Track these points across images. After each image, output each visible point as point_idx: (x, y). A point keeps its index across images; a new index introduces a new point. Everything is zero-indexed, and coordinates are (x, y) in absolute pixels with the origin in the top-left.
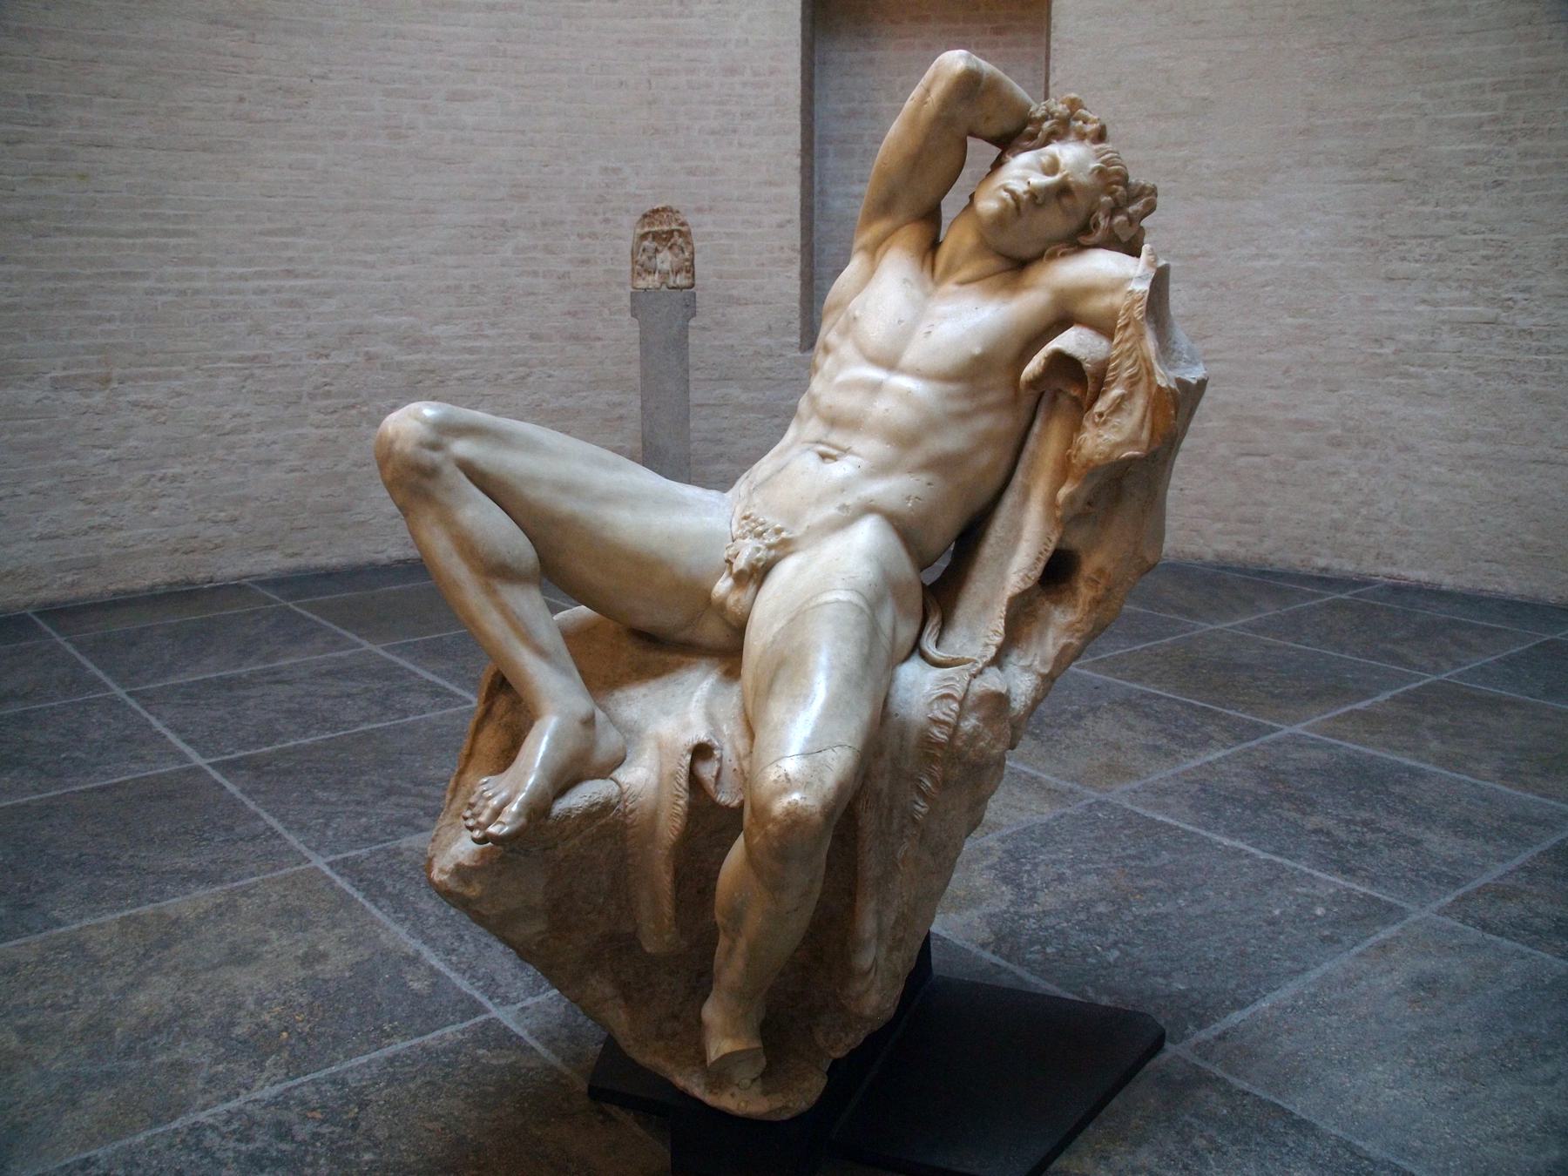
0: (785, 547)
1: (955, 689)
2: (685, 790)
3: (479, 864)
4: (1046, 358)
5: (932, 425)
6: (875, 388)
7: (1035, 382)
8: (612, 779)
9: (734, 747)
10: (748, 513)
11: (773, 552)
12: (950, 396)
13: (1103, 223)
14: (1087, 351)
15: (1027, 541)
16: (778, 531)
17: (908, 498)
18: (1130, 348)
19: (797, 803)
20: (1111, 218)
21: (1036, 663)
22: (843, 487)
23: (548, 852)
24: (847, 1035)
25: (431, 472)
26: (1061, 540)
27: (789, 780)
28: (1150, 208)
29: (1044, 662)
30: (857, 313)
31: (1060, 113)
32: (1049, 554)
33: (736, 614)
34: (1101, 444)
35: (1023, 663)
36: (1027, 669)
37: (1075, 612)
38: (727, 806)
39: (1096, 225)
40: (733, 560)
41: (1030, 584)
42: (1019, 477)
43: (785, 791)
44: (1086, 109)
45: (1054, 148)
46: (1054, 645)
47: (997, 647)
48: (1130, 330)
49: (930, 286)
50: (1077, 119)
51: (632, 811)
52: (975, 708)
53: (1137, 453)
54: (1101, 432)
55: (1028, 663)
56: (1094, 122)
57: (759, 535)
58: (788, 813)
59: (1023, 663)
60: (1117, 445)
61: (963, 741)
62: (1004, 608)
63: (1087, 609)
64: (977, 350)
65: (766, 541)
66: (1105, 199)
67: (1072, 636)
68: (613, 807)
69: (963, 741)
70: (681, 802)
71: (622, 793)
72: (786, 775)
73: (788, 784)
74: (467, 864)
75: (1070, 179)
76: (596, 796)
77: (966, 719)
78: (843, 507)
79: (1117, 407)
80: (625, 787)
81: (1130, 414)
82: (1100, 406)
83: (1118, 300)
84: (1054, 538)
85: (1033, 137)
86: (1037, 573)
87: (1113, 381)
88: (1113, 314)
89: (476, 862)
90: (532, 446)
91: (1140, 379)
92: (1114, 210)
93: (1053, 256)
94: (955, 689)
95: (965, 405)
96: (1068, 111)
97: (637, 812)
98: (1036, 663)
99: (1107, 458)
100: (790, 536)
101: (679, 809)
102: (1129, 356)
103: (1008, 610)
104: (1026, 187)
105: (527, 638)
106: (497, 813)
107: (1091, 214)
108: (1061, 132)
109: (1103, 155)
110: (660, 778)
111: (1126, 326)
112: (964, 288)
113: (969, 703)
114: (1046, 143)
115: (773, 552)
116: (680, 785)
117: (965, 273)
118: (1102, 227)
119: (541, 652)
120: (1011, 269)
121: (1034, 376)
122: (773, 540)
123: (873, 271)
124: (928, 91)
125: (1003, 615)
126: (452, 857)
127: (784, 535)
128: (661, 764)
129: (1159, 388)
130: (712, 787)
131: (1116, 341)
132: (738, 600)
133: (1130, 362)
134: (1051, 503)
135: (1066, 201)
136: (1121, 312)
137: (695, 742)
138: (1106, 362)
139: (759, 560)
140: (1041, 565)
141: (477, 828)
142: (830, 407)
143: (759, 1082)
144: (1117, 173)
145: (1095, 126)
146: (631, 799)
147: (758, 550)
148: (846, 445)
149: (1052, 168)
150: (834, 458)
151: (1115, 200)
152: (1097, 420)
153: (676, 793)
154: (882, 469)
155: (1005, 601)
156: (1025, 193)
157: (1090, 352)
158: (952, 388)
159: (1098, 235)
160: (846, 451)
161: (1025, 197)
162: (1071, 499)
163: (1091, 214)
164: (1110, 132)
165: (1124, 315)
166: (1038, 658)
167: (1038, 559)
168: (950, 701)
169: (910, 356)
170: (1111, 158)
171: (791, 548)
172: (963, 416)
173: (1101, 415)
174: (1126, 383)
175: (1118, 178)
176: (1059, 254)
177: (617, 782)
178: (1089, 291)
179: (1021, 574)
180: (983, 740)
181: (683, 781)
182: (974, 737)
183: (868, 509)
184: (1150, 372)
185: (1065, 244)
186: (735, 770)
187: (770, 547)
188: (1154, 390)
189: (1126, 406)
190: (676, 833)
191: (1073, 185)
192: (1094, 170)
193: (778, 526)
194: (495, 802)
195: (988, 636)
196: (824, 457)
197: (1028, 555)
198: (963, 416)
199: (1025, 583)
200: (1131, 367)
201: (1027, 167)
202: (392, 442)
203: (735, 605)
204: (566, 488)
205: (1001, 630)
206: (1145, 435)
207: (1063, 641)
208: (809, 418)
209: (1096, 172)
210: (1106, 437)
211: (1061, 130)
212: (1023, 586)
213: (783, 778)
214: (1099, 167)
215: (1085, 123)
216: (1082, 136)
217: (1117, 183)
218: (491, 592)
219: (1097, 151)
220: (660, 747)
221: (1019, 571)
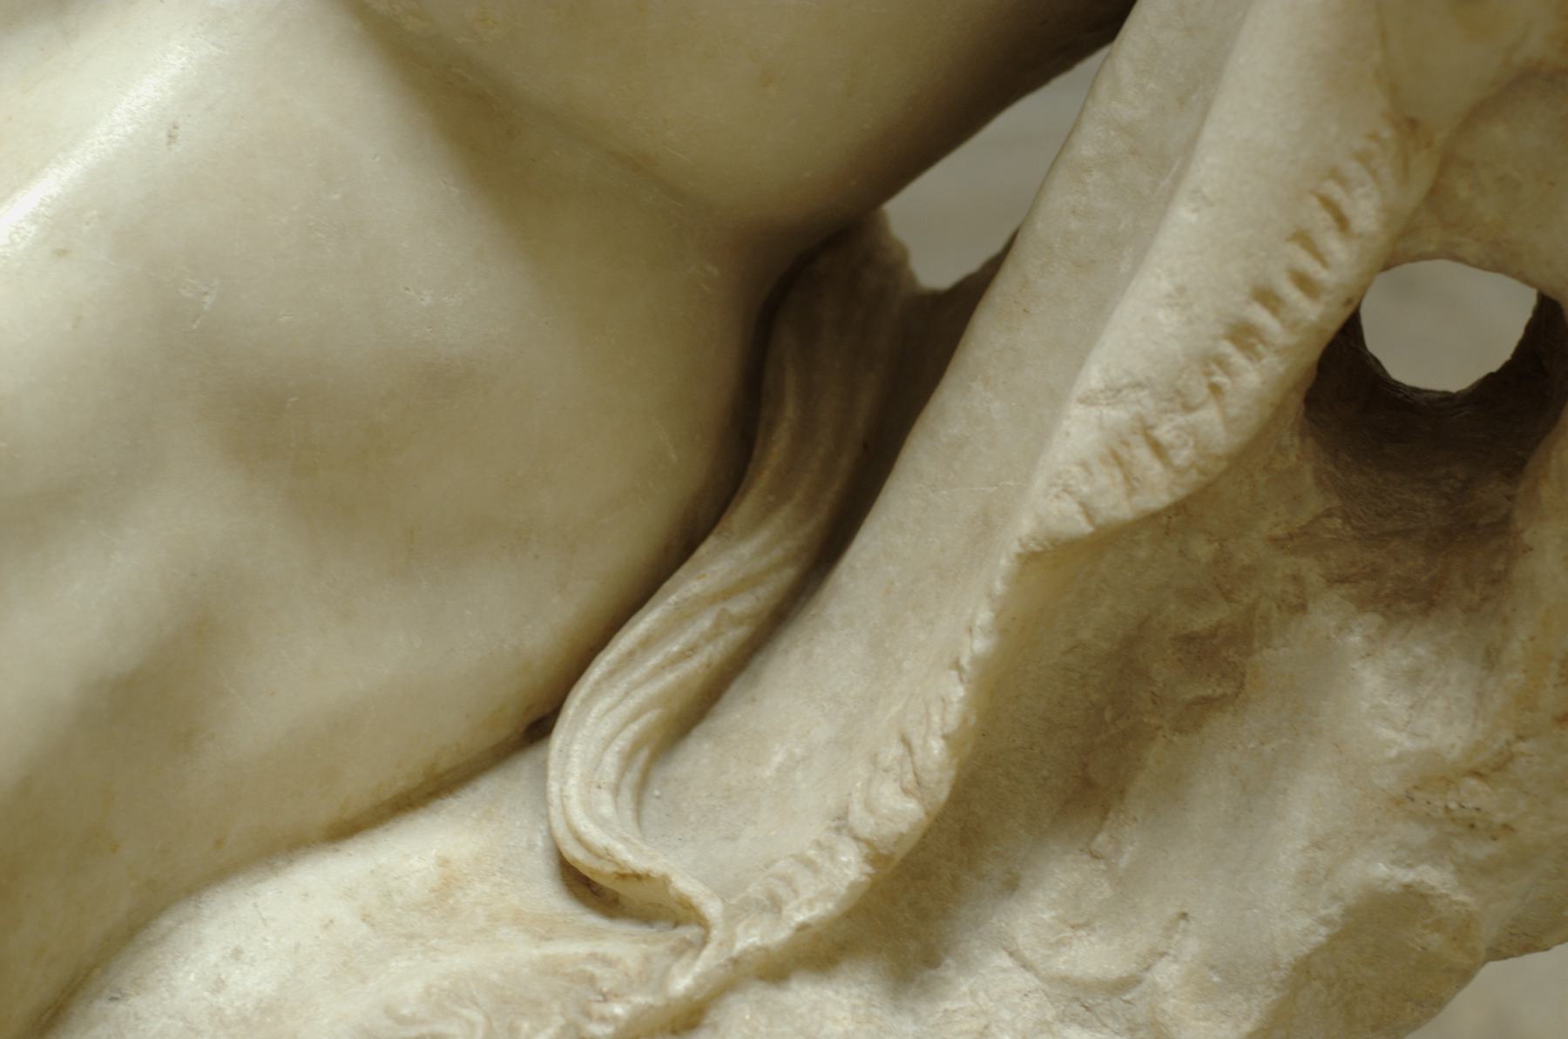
21: (1167, 974)
46: (1308, 879)
47: (876, 857)
55: (1116, 968)
62: (984, 616)
67: (1438, 851)
84: (1366, 212)
166: (1192, 947)
167: (1244, 335)
179: (1118, 415)
199: (1132, 483)
212: (1118, 506)
221: (1114, 393)
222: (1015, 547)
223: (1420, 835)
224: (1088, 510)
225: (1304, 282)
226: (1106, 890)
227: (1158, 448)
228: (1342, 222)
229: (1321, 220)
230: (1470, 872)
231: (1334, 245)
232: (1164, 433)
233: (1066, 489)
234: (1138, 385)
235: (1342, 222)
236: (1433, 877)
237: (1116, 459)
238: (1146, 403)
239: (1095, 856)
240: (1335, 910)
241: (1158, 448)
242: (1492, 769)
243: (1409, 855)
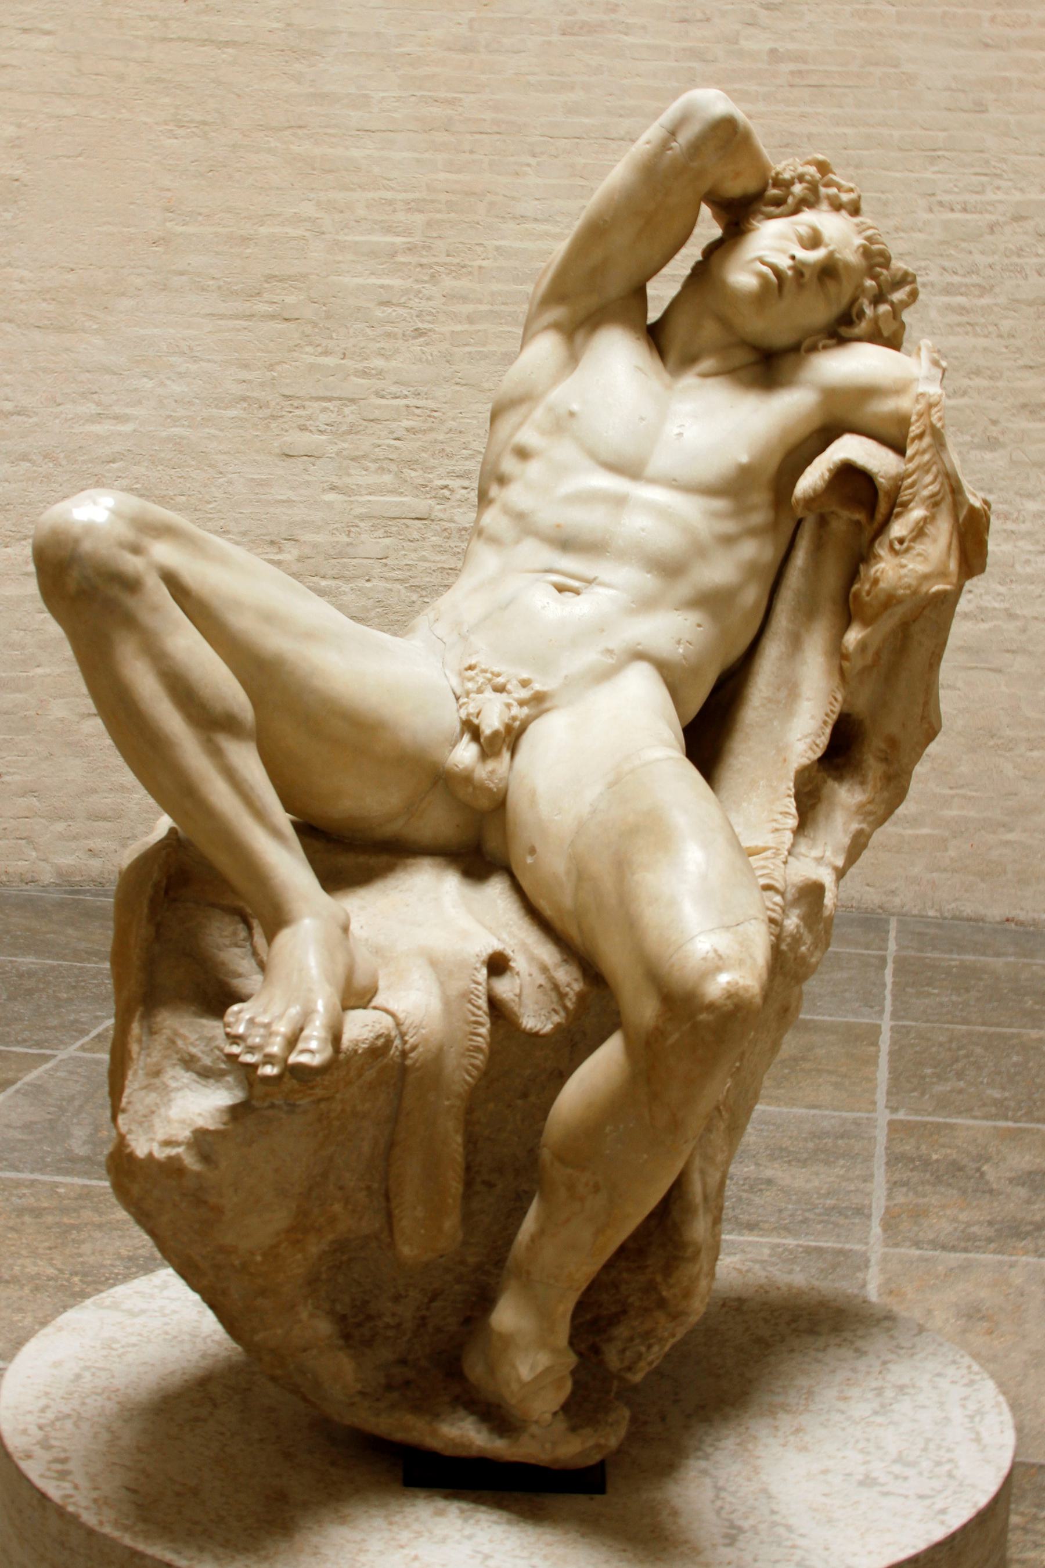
0: (539, 702)
1: (773, 878)
2: (485, 1012)
3: (229, 1127)
4: (830, 470)
5: (700, 551)
6: (620, 501)
7: (812, 501)
8: (375, 1008)
9: (532, 958)
10: (473, 662)
11: (525, 711)
12: (716, 515)
13: (869, 311)
15: (808, 699)
16: (525, 684)
17: (679, 642)
18: (928, 462)
19: (737, 983)
20: (875, 307)
22: (599, 628)
23: (323, 1106)
24: (649, 1347)
25: (131, 585)
26: (845, 701)
27: (720, 957)
28: (914, 295)
29: (835, 852)
30: (575, 407)
31: (812, 176)
32: (835, 717)
33: (490, 790)
34: (906, 576)
35: (816, 853)
36: (819, 860)
37: (864, 791)
38: (536, 1035)
39: (861, 314)
40: (476, 721)
41: (819, 754)
42: (782, 620)
43: (719, 969)
44: (835, 174)
45: (807, 217)
46: (845, 831)
48: (927, 440)
49: (666, 377)
50: (827, 185)
51: (414, 1048)
52: (796, 902)
53: (948, 587)
54: (904, 561)
56: (851, 190)
57: (500, 689)
58: (730, 996)
59: (816, 853)
60: (926, 577)
61: (788, 945)
62: (791, 785)
63: (879, 785)
64: (744, 459)
65: (516, 695)
66: (869, 283)
68: (392, 1042)
69: (788, 945)
70: (483, 1031)
71: (398, 1024)
72: (716, 951)
73: (719, 964)
74: (212, 1127)
75: (838, 256)
76: (378, 1026)
77: (788, 917)
78: (609, 652)
79: (919, 532)
80: (401, 1016)
81: (935, 541)
82: (898, 529)
83: (904, 404)
84: (840, 697)
85: (779, 202)
86: (824, 741)
87: (910, 501)
88: (903, 421)
89: (225, 1124)
90: (223, 560)
91: (943, 499)
92: (878, 299)
93: (813, 349)
94: (773, 878)
95: (730, 526)
96: (818, 176)
97: (420, 1049)
98: (828, 854)
99: (915, 593)
100: (545, 689)
101: (479, 1039)
102: (928, 471)
103: (795, 786)
104: (790, 262)
105: (260, 815)
106: (292, 1042)
107: (854, 301)
108: (808, 202)
109: (864, 230)
110: (446, 1002)
111: (921, 436)
112: (710, 381)
113: (789, 896)
114: (796, 211)
115: (525, 711)
116: (479, 1008)
117: (707, 364)
118: (867, 317)
119: (275, 833)
121: (815, 491)
122: (525, 694)
123: (573, 358)
124: (673, 133)
125: (792, 792)
126: (183, 1122)
127: (537, 686)
128: (442, 984)
129: (972, 509)
130: (516, 1009)
131: (909, 452)
132: (493, 772)
133: (929, 478)
134: (838, 653)
135: (831, 286)
136: (914, 418)
137: (490, 951)
138: (903, 477)
139: (514, 719)
140: (828, 731)
141: (265, 1063)
142: (558, 526)
143: (561, 1416)
144: (882, 254)
145: (852, 196)
146: (411, 1032)
147: (508, 706)
148: (590, 574)
149: (814, 241)
150: (577, 592)
151: (879, 285)
152: (897, 546)
153: (474, 1018)
154: (646, 604)
155: (792, 775)
156: (791, 268)
158: (720, 504)
159: (862, 327)
160: (590, 582)
161: (790, 273)
162: (863, 646)
163: (854, 301)
164: (864, 206)
165: (917, 421)
167: (825, 723)
168: (770, 893)
169: (660, 462)
170: (875, 234)
171: (547, 705)
172: (728, 540)
173: (901, 541)
174: (928, 502)
175: (881, 260)
176: (820, 345)
177: (387, 1011)
178: (867, 393)
179: (808, 740)
180: (805, 944)
181: (483, 1003)
182: (797, 940)
183: (639, 655)
184: (955, 489)
186: (541, 986)
187: (522, 703)
188: (963, 513)
189: (930, 529)
190: (475, 1073)
191: (841, 264)
192: (858, 248)
193: (525, 676)
194: (283, 1028)
195: (775, 820)
196: (561, 589)
197: (813, 717)
198: (728, 540)
199: (814, 752)
200: (932, 483)
201: (783, 237)
202: (77, 541)
203: (490, 779)
204: (269, 617)
205: (793, 811)
206: (953, 565)
207: (855, 826)
208: (517, 541)
209: (861, 250)
210: (911, 566)
211: (812, 198)
213: (711, 955)
214: (864, 246)
215: (839, 190)
216: (837, 206)
218: (216, 753)
219: (857, 225)
220: (434, 963)
221: (806, 737)
222: (794, 770)
223: (861, 817)
224: (808, 758)
225: (832, 711)
226: (810, 842)
227: (817, 745)
228: (836, 699)
229: (833, 700)
230: (869, 823)
231: (835, 703)
232: (818, 742)
233: (803, 756)
234: (810, 734)
235: (836, 699)
236: (864, 826)
237: (811, 749)
238: (813, 737)
239: (805, 836)
240: (851, 835)
241: (817, 745)
242: (870, 802)
243: (860, 822)
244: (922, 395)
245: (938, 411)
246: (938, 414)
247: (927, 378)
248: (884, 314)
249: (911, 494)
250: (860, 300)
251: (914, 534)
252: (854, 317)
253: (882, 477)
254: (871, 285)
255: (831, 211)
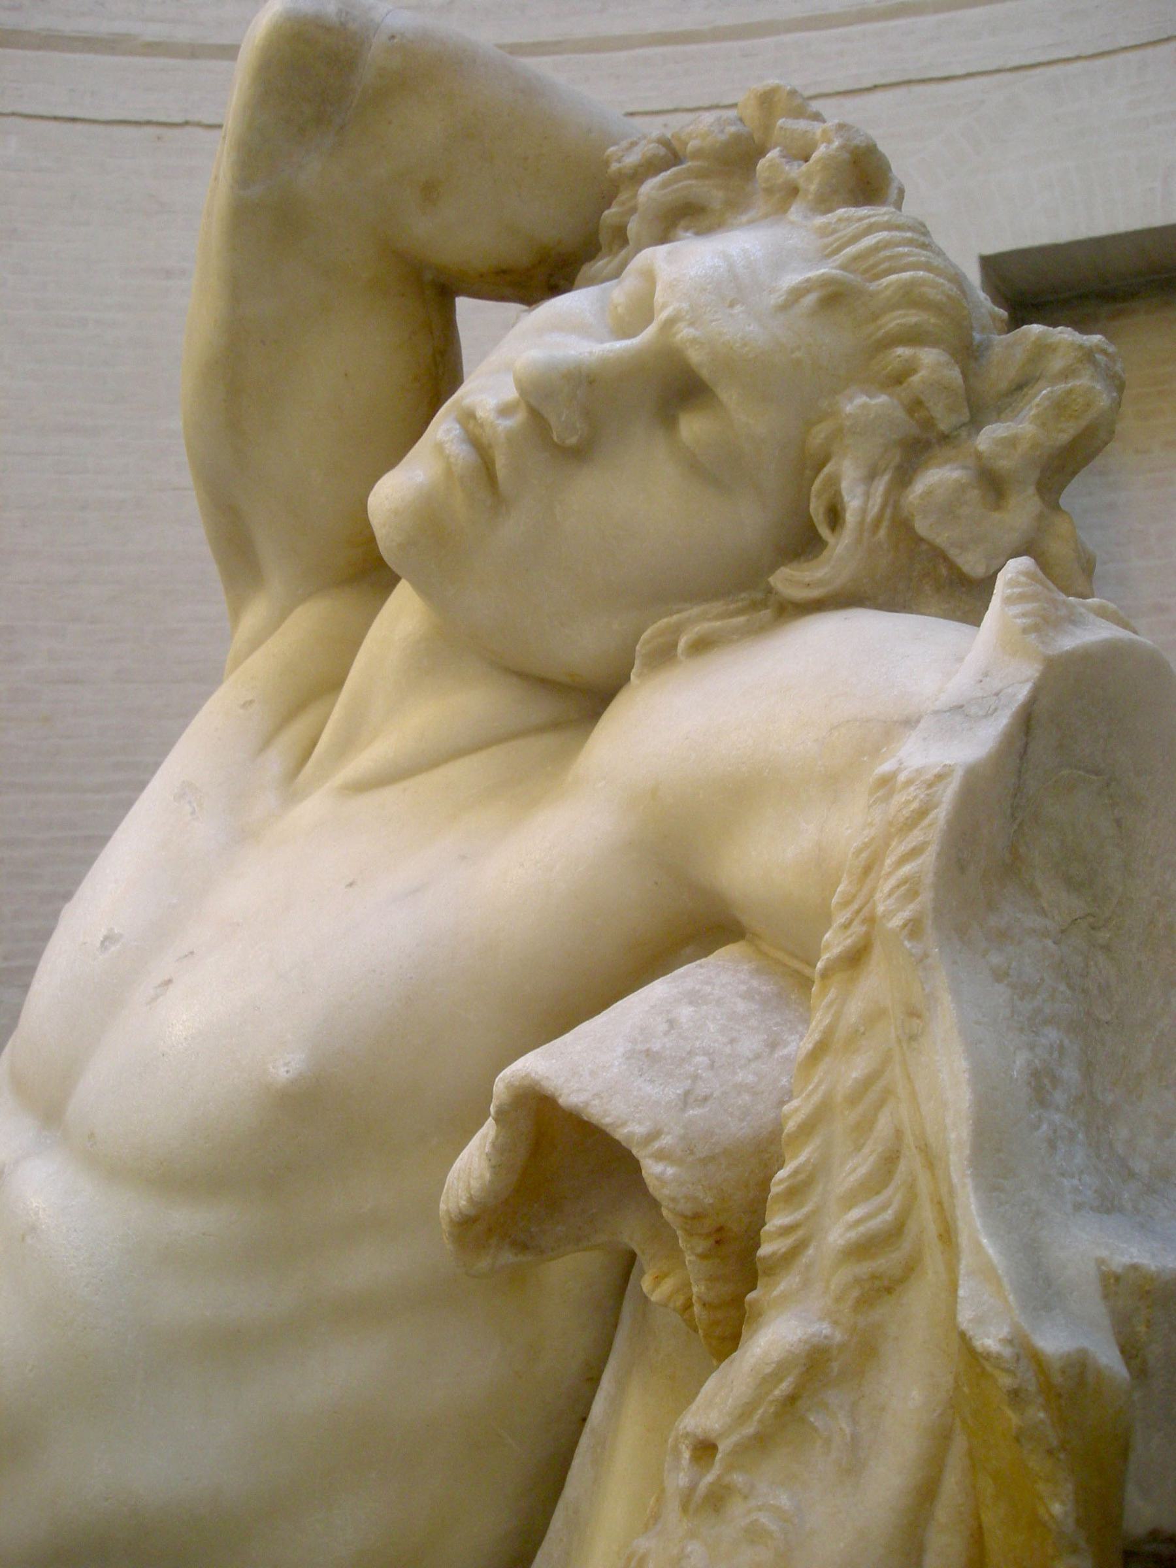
14: (673, 1091)
120: (540, 729)
151: (915, 405)
157: (686, 1099)
170: (887, 245)
185: (718, 606)
192: (797, 294)
209: (810, 299)
217: (914, 337)
219: (823, 232)
244: (886, 782)
245: (915, 852)
246: (906, 869)
247: (958, 708)
248: (929, 493)
249: (786, 1231)
250: (827, 470)
251: (750, 1429)
252: (824, 531)
253: (661, 1156)
254: (864, 406)
255: (766, 216)
